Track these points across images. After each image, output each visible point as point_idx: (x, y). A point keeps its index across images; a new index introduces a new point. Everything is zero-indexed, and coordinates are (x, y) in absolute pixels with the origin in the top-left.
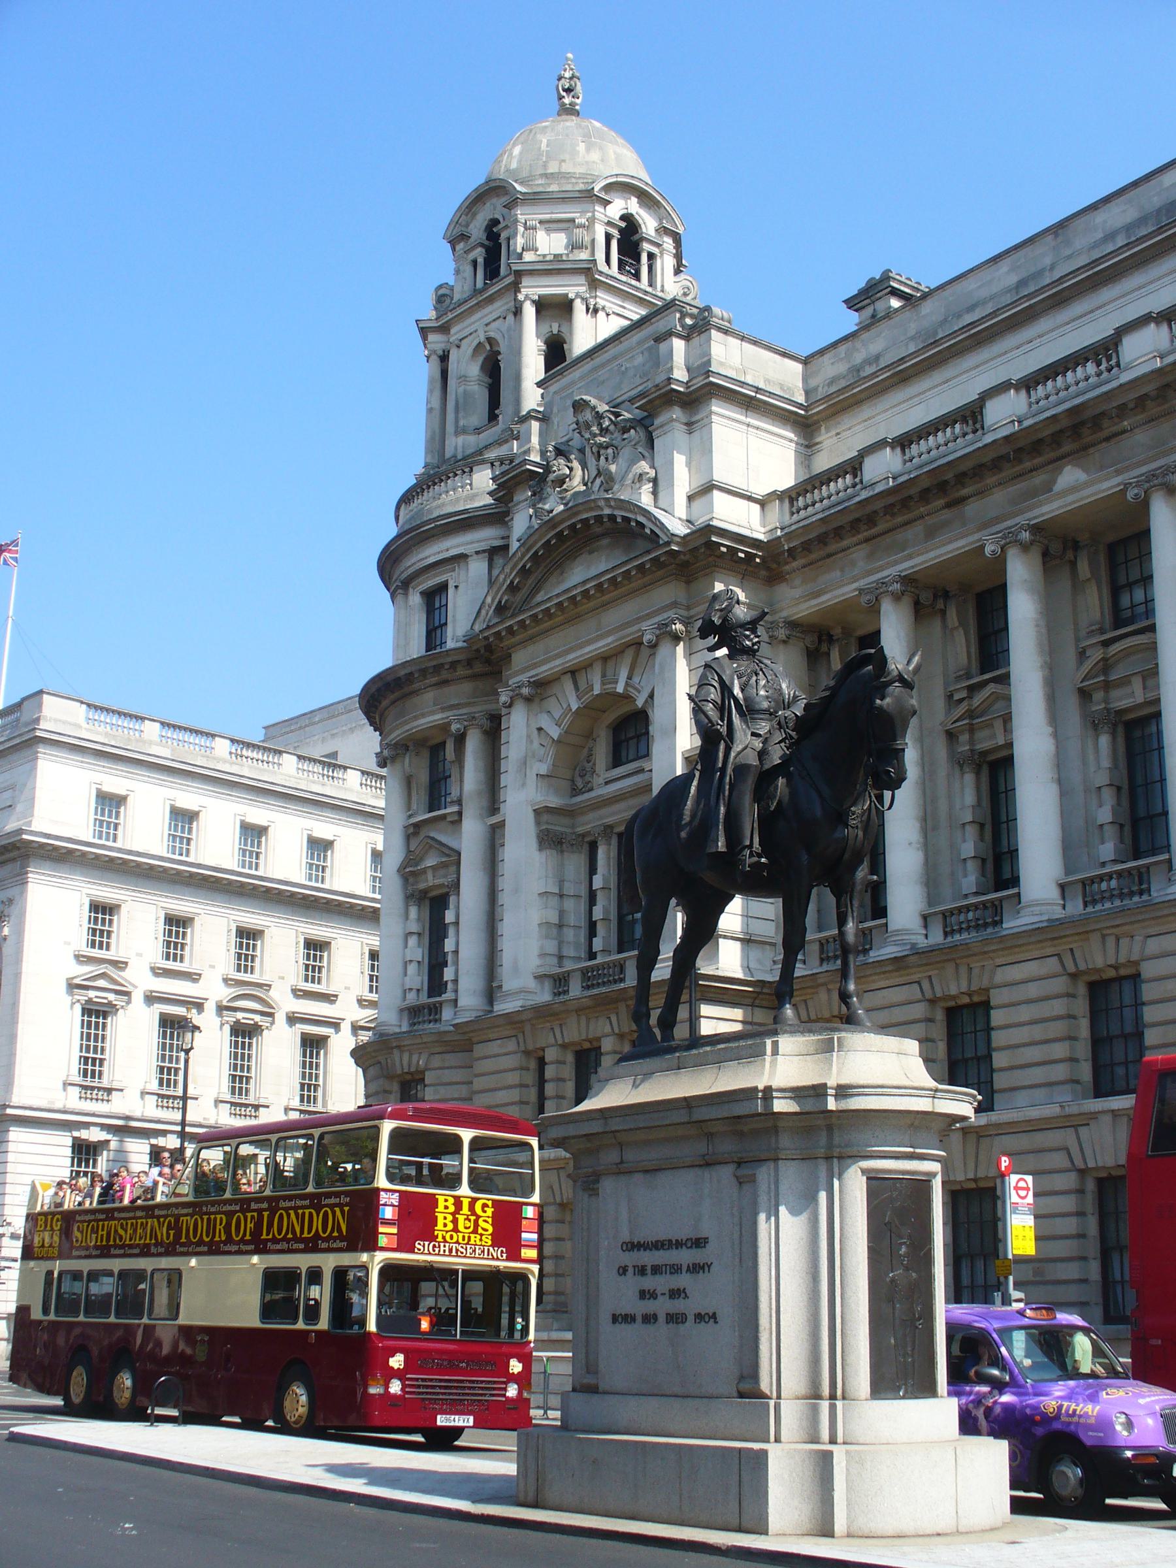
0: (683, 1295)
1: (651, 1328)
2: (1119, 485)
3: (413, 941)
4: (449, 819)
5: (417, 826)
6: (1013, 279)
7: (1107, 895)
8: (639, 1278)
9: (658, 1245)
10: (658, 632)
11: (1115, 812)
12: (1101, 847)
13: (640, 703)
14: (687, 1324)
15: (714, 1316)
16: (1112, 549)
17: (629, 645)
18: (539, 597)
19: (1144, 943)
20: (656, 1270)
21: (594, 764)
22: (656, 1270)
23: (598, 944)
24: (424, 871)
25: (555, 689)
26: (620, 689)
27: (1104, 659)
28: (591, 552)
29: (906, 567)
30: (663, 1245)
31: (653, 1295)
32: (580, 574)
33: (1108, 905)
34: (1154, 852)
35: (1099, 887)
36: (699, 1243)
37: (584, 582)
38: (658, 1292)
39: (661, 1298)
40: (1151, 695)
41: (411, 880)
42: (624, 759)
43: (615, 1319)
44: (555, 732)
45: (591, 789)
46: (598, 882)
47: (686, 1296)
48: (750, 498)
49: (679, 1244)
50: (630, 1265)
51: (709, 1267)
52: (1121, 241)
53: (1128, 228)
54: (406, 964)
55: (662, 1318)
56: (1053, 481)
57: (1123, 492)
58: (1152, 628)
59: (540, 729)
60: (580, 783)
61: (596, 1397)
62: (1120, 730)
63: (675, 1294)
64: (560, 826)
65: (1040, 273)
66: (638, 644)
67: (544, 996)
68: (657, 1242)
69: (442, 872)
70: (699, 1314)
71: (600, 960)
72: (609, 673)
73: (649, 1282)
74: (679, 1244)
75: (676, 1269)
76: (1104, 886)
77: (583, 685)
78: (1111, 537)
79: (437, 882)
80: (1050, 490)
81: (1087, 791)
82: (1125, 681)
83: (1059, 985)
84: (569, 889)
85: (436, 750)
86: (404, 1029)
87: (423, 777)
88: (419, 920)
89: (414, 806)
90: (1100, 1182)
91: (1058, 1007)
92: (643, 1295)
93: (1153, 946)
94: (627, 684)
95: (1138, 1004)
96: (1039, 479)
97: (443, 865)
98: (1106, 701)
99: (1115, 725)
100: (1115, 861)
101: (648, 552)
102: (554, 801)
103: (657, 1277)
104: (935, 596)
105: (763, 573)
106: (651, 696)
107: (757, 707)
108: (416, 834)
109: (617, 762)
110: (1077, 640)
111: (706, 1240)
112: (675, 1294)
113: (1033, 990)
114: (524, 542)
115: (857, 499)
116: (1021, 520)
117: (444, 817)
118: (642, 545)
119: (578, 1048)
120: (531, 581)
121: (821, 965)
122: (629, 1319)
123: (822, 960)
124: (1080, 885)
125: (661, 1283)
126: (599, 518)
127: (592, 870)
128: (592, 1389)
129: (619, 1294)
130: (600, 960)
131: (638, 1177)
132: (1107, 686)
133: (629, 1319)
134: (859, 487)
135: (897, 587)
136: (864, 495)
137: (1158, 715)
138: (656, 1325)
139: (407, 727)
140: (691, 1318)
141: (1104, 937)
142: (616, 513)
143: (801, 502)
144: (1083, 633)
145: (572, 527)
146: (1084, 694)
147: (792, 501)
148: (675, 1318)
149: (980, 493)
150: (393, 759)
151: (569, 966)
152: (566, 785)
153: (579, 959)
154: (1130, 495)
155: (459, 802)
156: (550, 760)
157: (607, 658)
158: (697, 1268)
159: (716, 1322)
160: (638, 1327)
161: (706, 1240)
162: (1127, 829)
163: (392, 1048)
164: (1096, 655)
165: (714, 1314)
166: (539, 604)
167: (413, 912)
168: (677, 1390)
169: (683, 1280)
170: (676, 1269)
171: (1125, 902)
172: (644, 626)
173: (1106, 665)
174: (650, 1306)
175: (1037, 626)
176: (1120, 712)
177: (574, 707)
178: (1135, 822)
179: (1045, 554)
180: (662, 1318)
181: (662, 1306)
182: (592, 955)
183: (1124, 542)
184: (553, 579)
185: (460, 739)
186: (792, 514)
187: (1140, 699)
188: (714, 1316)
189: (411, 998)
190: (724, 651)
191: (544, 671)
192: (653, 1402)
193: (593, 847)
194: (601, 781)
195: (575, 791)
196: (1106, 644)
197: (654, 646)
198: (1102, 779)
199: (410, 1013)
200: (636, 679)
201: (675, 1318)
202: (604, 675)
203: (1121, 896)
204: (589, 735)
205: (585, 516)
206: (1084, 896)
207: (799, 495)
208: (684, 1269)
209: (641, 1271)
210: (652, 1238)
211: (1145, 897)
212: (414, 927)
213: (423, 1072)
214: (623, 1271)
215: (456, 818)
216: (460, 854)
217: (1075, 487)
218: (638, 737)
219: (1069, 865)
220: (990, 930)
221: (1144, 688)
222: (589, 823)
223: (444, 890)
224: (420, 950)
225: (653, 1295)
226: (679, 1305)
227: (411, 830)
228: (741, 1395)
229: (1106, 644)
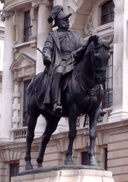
3: (16, 101)
4: (32, 46)
5: (18, 48)
21: (93, 23)
24: (21, 69)
41: (15, 73)
54: (13, 111)
59: (69, 7)
69: (28, 70)
79: (27, 74)
85: (27, 14)
86: (12, 140)
87: (21, 26)
88: (19, 91)
89: (17, 40)
97: (29, 67)
107: (65, 50)
108: (17, 52)
117: (29, 45)
119: (83, 151)
139: (13, 3)
150: (8, 17)
155: (36, 38)
163: (6, 149)
167: (16, 87)
185: (37, 9)
189: (15, 127)
194: (95, 31)
199: (14, 133)
204: (90, 10)
212: (17, 94)
213: (19, 160)
215: (34, 45)
216: (35, 62)
223: (30, 78)
224: (19, 105)
227: (15, 50)
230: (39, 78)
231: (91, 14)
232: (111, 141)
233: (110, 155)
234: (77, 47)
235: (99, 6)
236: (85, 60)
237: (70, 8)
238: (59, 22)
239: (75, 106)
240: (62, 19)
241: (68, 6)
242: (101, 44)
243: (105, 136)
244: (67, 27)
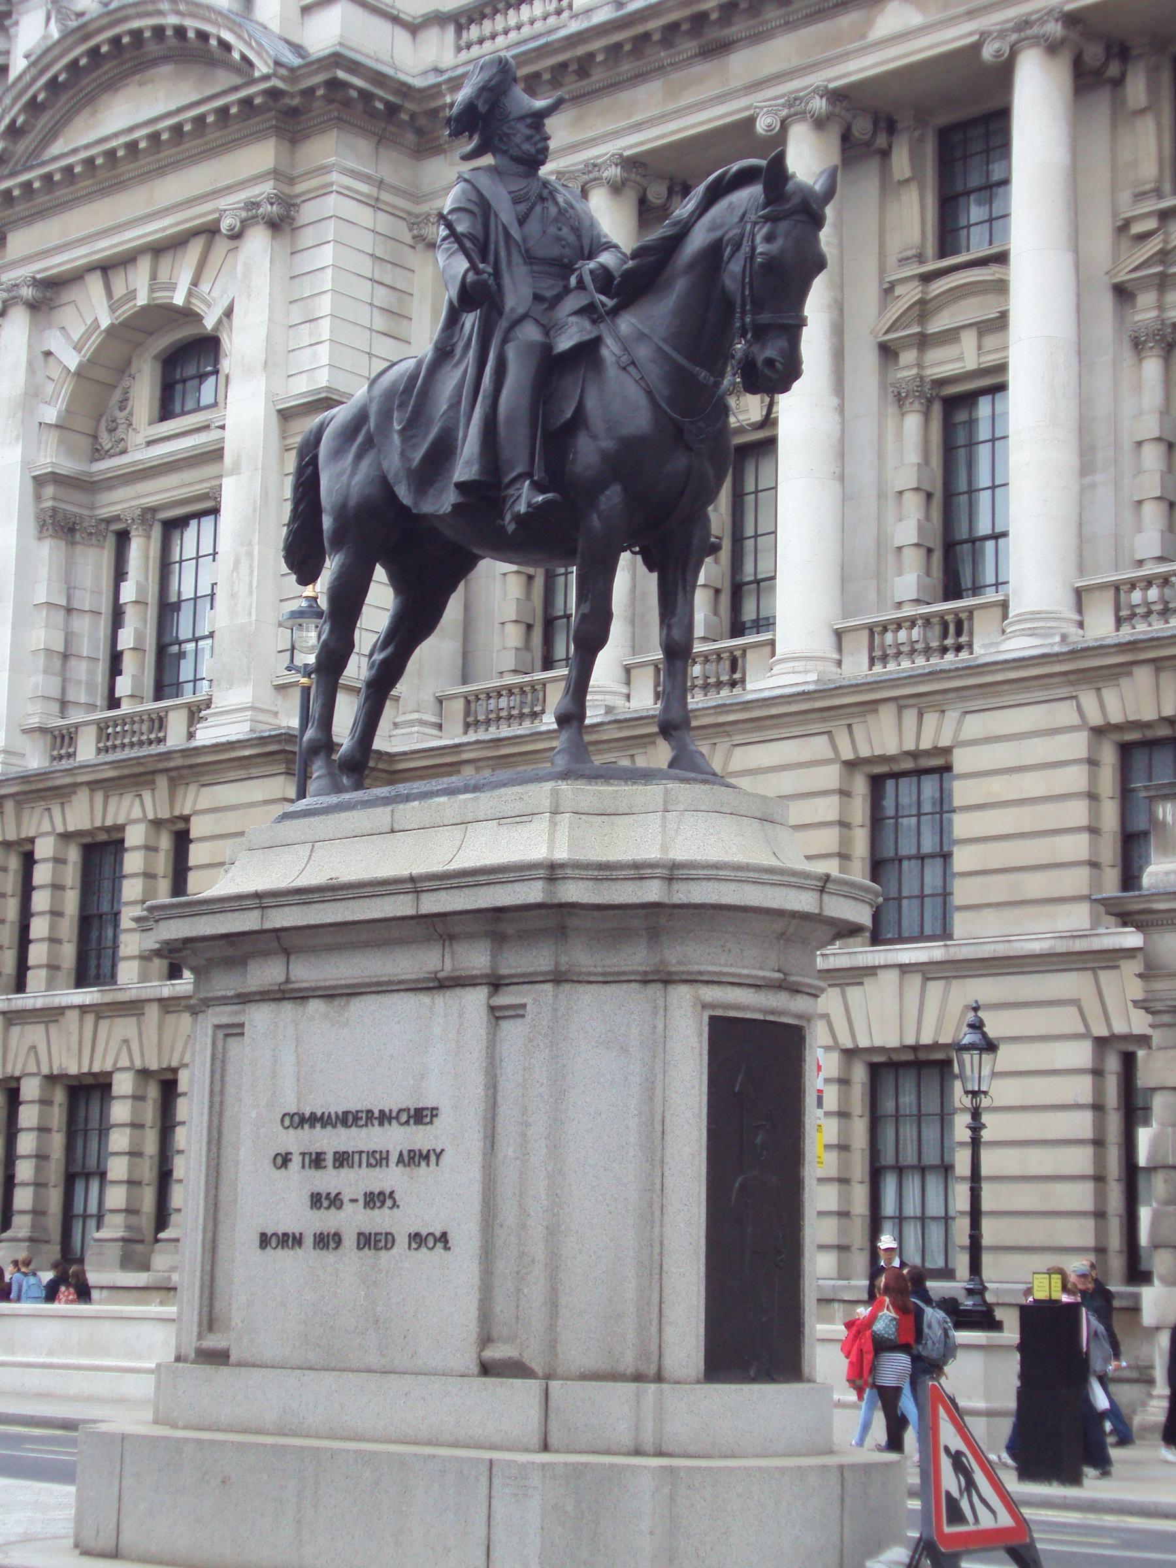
0: (389, 1203)
1: (329, 1257)
2: (971, 34)
7: (905, 649)
8: (312, 1173)
9: (348, 1119)
10: (244, 214)
11: (921, 530)
12: (897, 579)
13: (209, 323)
14: (394, 1251)
15: (443, 1239)
16: (945, 136)
17: (195, 233)
18: (56, 148)
19: (960, 722)
20: (342, 1159)
21: (131, 414)
22: (342, 1159)
23: (124, 686)
25: (73, 294)
26: (179, 299)
27: (922, 302)
28: (141, 84)
29: (633, 143)
30: (356, 1118)
31: (335, 1201)
32: (125, 113)
33: (906, 664)
34: (976, 590)
35: (895, 638)
36: (420, 1116)
37: (131, 129)
38: (346, 1198)
39: (348, 1207)
40: (989, 360)
42: (178, 409)
43: (265, 1240)
44: (72, 361)
45: (124, 452)
46: (128, 593)
47: (395, 1205)
48: (396, 20)
49: (384, 1118)
50: (295, 1150)
51: (438, 1156)
55: (349, 1241)
56: (869, 23)
57: (976, 47)
58: (1002, 258)
59: (48, 354)
60: (106, 441)
61: (224, 1371)
62: (937, 409)
63: (375, 1200)
64: (74, 505)
66: (211, 231)
67: (35, 760)
68: (346, 1113)
70: (417, 1235)
71: (126, 708)
72: (163, 276)
73: (330, 1180)
74: (384, 1118)
75: (379, 1159)
76: (902, 635)
77: (119, 290)
78: (944, 118)
80: (863, 36)
81: (881, 496)
82: (951, 336)
84: (84, 600)
90: (874, 1070)
92: (316, 1200)
93: (975, 726)
94: (190, 293)
95: (944, 808)
98: (920, 366)
99: (930, 401)
100: (917, 601)
101: (236, 89)
102: (68, 466)
103: (345, 1171)
104: (671, 191)
105: (410, 137)
106: (229, 313)
109: (166, 412)
110: (882, 271)
111: (434, 1112)
112: (375, 1200)
114: (39, 62)
115: (562, 33)
116: (817, 79)
118: (225, 79)
119: (88, 840)
120: (44, 121)
121: (466, 733)
122: (290, 1240)
123: (467, 726)
125: (350, 1182)
126: (159, 31)
127: (120, 575)
128: (218, 1357)
129: (281, 1200)
130: (126, 708)
131: (316, 1007)
132: (923, 342)
133: (290, 1240)
134: (566, 14)
135: (614, 172)
136: (575, 26)
137: (1002, 387)
138: (341, 1251)
140: (402, 1241)
141: (900, 709)
142: (189, 23)
143: (474, 32)
144: (892, 261)
145: (116, 41)
146: (888, 352)
147: (459, 29)
148: (368, 1241)
149: (757, 38)
151: (76, 716)
152: (84, 443)
153: (92, 707)
154: (987, 53)
156: (61, 404)
157: (161, 249)
158: (414, 1158)
159: (447, 1248)
160: (307, 1254)
161: (434, 1112)
162: (937, 557)
164: (909, 294)
165: (444, 1235)
166: (55, 159)
168: (373, 1360)
169: (390, 1178)
170: (379, 1159)
171: (933, 661)
172: (223, 203)
173: (923, 309)
174: (328, 1220)
176: (940, 383)
177: (105, 323)
178: (950, 547)
179: (846, 137)
180: (349, 1241)
181: (352, 1220)
182: (113, 702)
183: (963, 126)
184: (79, 122)
186: (459, 49)
187: (971, 364)
188: (443, 1239)
190: (488, 160)
191: (58, 263)
192: (329, 1380)
193: (123, 537)
194: (140, 439)
195: (97, 453)
196: (927, 278)
197: (236, 236)
198: (906, 477)
200: (204, 287)
201: (368, 1241)
202: (154, 277)
203: (927, 651)
204: (123, 369)
205: (136, 24)
206: (871, 648)
207: (471, 21)
208: (394, 1158)
209: (316, 1161)
210: (336, 1106)
211: (964, 655)
214: (283, 1160)
218: (202, 377)
219: (847, 599)
220: (725, 692)
221: (979, 348)
222: (121, 502)
225: (335, 1201)
226: (379, 1220)
228: (486, 1369)
229: (927, 278)
230: (413, 378)
231: (126, 382)
232: (203, 804)
233: (197, 854)
234: (586, 251)
235: (155, 358)
236: (680, 286)
237: (51, 359)
238: (507, 131)
239: (612, 497)
240: (522, 118)
241: (45, 349)
242: (796, 200)
243: (180, 791)
244: (541, 157)
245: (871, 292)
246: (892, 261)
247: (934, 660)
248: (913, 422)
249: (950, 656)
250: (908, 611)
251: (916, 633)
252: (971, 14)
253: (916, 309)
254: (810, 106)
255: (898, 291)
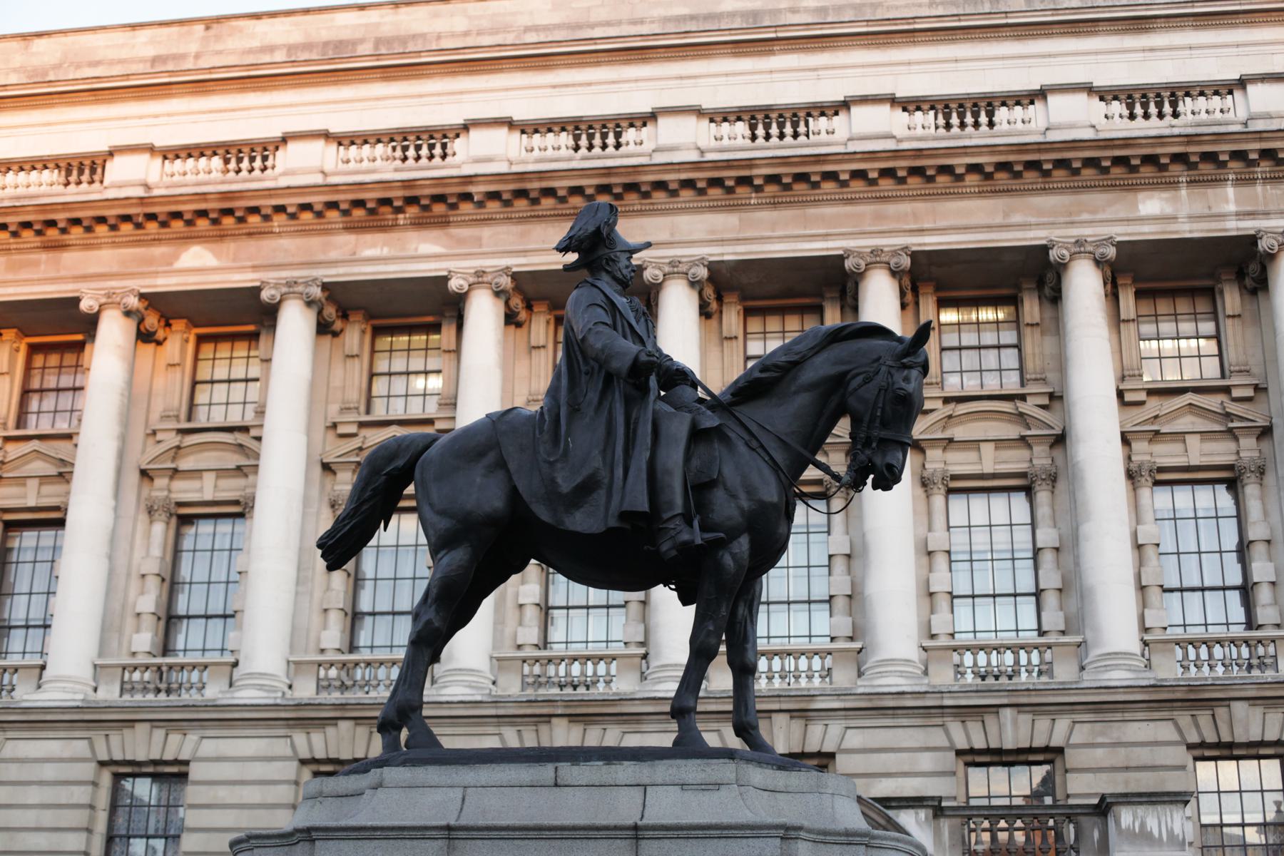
6: (151, 52)
11: (157, 605)
12: (135, 636)
27: (178, 448)
52: (280, 56)
53: (291, 48)
56: (176, 257)
65: (183, 57)
80: (171, 264)
82: (196, 473)
83: (87, 771)
91: (81, 795)
96: (159, 251)
113: (49, 772)
124: (120, 670)
164: (172, 440)
175: (122, 395)
176: (180, 504)
217: (199, 266)
221: (216, 486)
245: (138, 433)
246: (155, 416)
247: (150, 697)
248: (159, 528)
249: (162, 696)
250: (141, 659)
251: (147, 676)
252: (255, 268)
253: (172, 453)
254: (124, 301)
255: (159, 436)
